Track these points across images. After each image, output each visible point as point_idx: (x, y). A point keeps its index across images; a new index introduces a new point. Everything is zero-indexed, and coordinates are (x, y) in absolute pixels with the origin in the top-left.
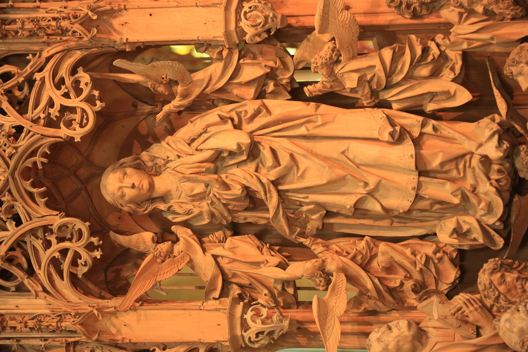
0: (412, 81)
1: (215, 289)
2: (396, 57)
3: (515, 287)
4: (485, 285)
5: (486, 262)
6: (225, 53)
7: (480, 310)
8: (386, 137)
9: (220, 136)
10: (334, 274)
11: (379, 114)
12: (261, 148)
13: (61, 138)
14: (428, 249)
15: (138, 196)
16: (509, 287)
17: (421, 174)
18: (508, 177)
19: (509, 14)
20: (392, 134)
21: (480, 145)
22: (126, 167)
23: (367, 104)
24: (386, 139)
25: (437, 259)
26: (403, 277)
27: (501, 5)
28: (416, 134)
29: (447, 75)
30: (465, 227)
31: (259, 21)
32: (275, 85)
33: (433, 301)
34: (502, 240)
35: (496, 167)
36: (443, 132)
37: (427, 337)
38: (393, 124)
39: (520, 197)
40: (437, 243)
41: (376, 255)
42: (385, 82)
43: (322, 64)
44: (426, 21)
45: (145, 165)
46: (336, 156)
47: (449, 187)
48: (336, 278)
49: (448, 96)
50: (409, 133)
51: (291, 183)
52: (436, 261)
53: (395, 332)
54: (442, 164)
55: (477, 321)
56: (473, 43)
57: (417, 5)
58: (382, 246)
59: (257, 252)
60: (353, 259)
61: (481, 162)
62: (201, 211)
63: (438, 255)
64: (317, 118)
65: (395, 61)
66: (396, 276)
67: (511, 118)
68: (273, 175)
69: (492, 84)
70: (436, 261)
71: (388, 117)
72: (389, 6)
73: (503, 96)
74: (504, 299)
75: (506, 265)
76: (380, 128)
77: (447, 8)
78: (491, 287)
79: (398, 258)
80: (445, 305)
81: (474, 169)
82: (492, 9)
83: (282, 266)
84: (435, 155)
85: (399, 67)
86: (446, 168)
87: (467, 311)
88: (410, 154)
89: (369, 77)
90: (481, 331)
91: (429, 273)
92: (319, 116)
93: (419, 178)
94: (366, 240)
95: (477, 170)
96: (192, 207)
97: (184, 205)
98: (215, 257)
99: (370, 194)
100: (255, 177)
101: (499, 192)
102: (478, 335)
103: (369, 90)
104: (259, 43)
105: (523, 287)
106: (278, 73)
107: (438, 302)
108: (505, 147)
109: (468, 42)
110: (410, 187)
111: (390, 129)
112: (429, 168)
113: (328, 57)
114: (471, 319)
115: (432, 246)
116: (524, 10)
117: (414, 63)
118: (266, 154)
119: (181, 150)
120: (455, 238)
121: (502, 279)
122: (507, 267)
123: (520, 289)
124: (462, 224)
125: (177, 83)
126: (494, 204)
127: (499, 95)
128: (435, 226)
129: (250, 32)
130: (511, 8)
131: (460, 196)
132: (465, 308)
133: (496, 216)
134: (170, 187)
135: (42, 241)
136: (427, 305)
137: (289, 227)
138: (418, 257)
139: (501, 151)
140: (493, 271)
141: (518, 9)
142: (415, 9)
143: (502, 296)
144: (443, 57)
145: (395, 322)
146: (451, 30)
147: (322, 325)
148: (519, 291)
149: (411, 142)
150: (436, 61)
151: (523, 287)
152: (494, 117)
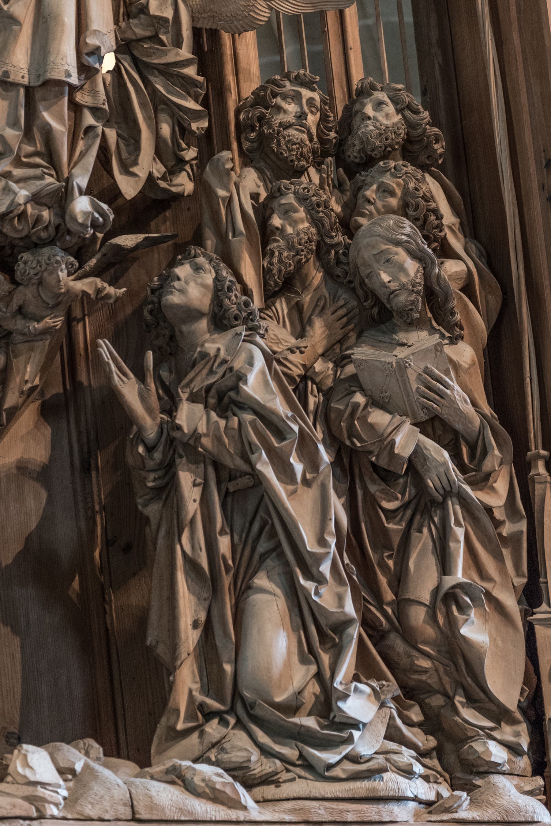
27: (286, 254)
29: (158, 169)
130: (283, 268)
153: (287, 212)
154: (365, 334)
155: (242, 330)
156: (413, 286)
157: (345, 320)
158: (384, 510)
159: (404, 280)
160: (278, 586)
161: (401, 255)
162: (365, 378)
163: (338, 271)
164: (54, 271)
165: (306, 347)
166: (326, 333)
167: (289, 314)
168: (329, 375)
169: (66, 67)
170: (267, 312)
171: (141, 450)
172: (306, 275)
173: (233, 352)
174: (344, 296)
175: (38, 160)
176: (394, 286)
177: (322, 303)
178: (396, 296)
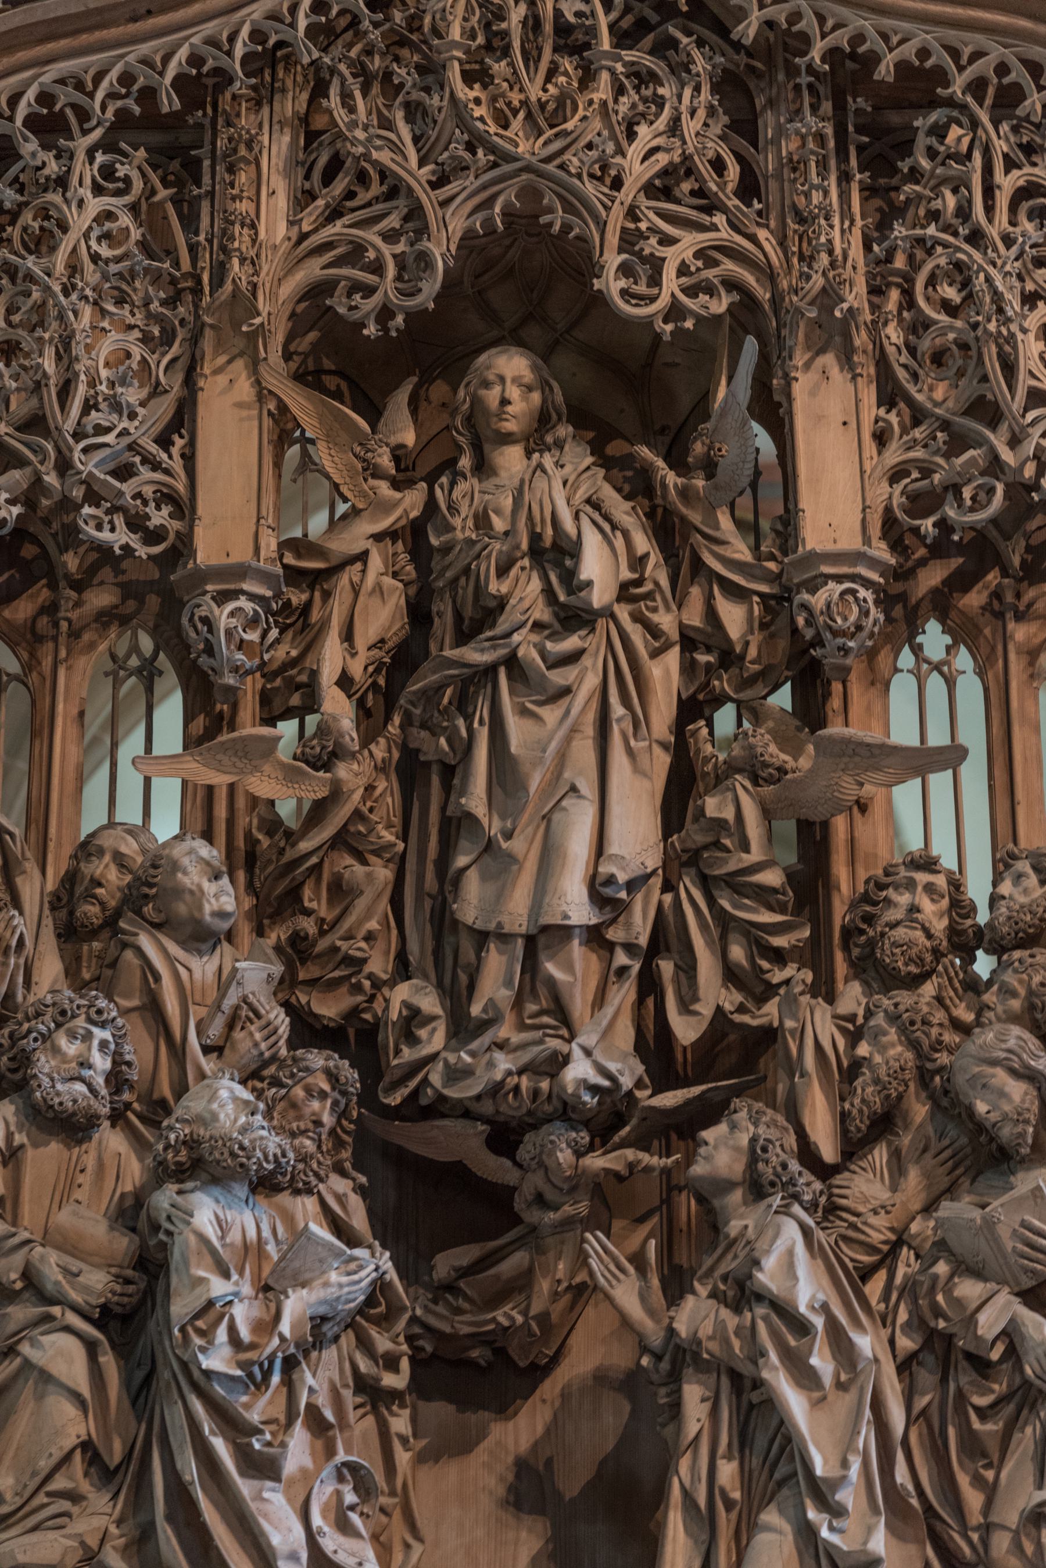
0: (720, 930)
1: (299, 556)
2: (764, 896)
3: (299, 1118)
4: (304, 1059)
5: (352, 1066)
6: (772, 565)
7: (255, 1052)
8: (605, 869)
9: (607, 549)
10: (328, 775)
11: (653, 861)
12: (583, 633)
13: (601, 254)
14: (378, 965)
15: (486, 412)
16: (300, 1103)
17: (530, 941)
18: (524, 1110)
19: (852, 1105)
20: (611, 880)
21: (588, 1053)
22: (543, 393)
23: (672, 843)
24: (601, 869)
25: (359, 982)
26: (323, 913)
27: (870, 1090)
28: (614, 934)
29: (731, 999)
30: (423, 1033)
31: (839, 621)
32: (708, 663)
33: (272, 963)
34: (398, 1100)
35: (545, 1085)
36: (616, 986)
37: (200, 953)
38: (631, 886)
39: (485, 1135)
40: (392, 983)
41: (364, 862)
42: (717, 873)
43: (751, 747)
44: (839, 956)
45: (547, 431)
46: (567, 775)
47: (504, 995)
48: (319, 778)
49: (687, 999)
50: (614, 921)
51: (512, 692)
52: (353, 980)
53: (209, 888)
54: (551, 983)
55: (233, 1048)
56: (794, 1040)
57: (871, 933)
58: (384, 874)
60: (357, 815)
61: (555, 1053)
62: (455, 529)
63: (367, 984)
64: (644, 740)
66: (324, 901)
67: (644, 1119)
68: (529, 653)
69: (710, 1085)
70: (353, 980)
71: (649, 876)
72: (867, 882)
73: (688, 1103)
74: (279, 1096)
75: (347, 1105)
76: (623, 858)
77: (864, 993)
79: (361, 905)
80: (264, 985)
81: (541, 1042)
82: (864, 1074)
83: (344, 681)
84: (569, 968)
85: (746, 901)
86: (542, 991)
87: (253, 1028)
88: (570, 914)
89: (727, 842)
90: (215, 1054)
91: (331, 966)
92: (647, 743)
93: (522, 936)
95: (536, 1049)
96: (463, 515)
97: (467, 501)
98: (363, 557)
99: (490, 846)
100: (524, 618)
101: (496, 1090)
102: (207, 1050)
103: (699, 845)
104: (795, 631)
105: (303, 1132)
106: (734, 671)
108: (587, 1098)
109: (796, 1029)
110: (505, 919)
111: (622, 877)
112: (542, 956)
113: (767, 758)
114: (238, 1035)
115: (386, 972)
116: (860, 1135)
117: (753, 930)
118: (572, 642)
119: (578, 488)
120: (400, 1012)
122: (342, 1106)
123: (298, 1127)
124: (429, 1027)
125: (710, 477)
126: (468, 1082)
127: (691, 1096)
128: (426, 977)
129: (818, 600)
131: (485, 1016)
133: (444, 1087)
134: (503, 474)
135: (398, 227)
136: (266, 954)
137: (424, 692)
138: (363, 945)
139: (577, 1088)
140: (332, 1077)
141: (861, 1121)
142: (862, 932)
143: (283, 1091)
144: (767, 991)
145: (230, 889)
146: (820, 1000)
147: (224, 747)
148: (294, 1125)
149: (594, 921)
150: (757, 976)
152: (646, 1087)
153: (878, 1033)
154: (980, 1178)
155: (777, 1201)
156: (1019, 1114)
157: (950, 1163)
158: (977, 1409)
159: (1007, 1108)
160: (789, 1521)
161: (1001, 1077)
162: (953, 1242)
163: (945, 1102)
165: (893, 1205)
167: (888, 1162)
168: (928, 1237)
170: (861, 1163)
171: (645, 1361)
172: (907, 1111)
173: (760, 1232)
174: (952, 1132)
176: (994, 1117)
177: (922, 1146)
178: (1000, 1128)
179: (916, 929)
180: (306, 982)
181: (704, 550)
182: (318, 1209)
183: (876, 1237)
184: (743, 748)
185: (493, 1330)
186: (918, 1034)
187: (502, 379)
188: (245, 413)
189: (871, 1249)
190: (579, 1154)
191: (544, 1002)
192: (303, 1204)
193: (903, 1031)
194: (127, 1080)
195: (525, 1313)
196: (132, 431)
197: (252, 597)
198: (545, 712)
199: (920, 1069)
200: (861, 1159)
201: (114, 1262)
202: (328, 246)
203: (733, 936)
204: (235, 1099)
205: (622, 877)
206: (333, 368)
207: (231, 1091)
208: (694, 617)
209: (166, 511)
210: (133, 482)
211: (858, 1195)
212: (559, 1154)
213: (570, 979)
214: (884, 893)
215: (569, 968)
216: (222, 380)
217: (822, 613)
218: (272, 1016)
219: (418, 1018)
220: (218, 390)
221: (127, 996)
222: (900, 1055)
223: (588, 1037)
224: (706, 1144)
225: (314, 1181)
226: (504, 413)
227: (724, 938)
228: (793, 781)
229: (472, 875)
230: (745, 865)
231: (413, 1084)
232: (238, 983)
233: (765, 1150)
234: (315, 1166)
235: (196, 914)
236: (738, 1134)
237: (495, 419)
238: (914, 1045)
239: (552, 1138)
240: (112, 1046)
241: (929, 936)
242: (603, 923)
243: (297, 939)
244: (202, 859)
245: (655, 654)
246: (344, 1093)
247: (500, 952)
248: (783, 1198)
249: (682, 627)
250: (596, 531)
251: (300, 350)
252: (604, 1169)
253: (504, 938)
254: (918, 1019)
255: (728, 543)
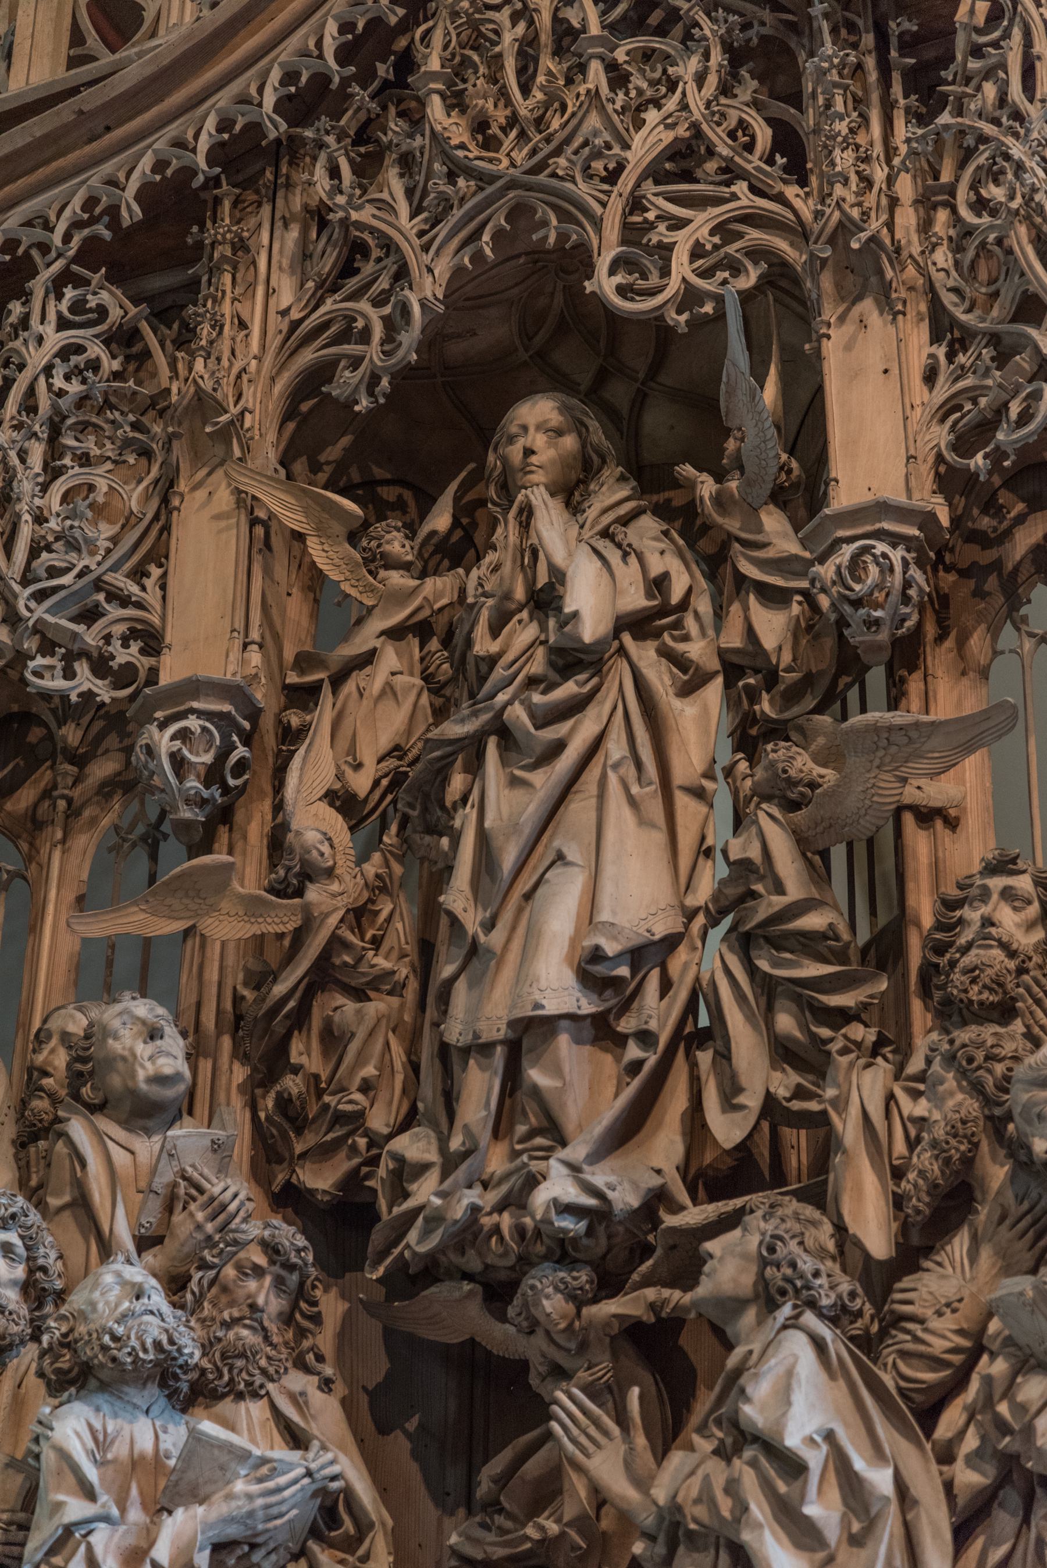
3: (232, 1304)
7: (200, 1236)
16: (231, 1285)
37: (148, 1132)
46: (556, 844)
53: (143, 1050)
54: (536, 1092)
59: (385, 742)
60: (335, 942)
65: (804, 945)
67: (674, 1247)
68: (518, 713)
75: (301, 1284)
78: (227, 1245)
80: (210, 1154)
84: (557, 1070)
85: (788, 955)
88: (544, 1002)
93: (502, 1042)
94: (394, 972)
105: (236, 1321)
107: (215, 1138)
110: (482, 1026)
112: (525, 1063)
114: (178, 1218)
117: (799, 990)
121: (252, 1269)
130: (921, 1182)
132: (202, 1199)
140: (271, 1248)
141: (919, 1200)
143: (212, 1273)
148: (226, 1315)
150: (820, 1050)
151: (236, 1321)
155: (787, 1310)
164: (538, 1304)
165: (960, 1300)
166: (999, 1265)
169: (537, 996)
175: (539, 1141)
179: (991, 947)
180: (303, 1155)
181: (741, 559)
182: (268, 1414)
183: (938, 1346)
184: (766, 769)
185: (530, 1550)
186: (981, 1072)
187: (525, 428)
188: (223, 524)
189: (935, 1362)
190: (579, 1300)
191: (533, 1120)
192: (248, 1410)
193: (963, 1073)
194: (44, 1289)
195: (558, 1521)
196: (93, 567)
197: (208, 715)
198: (537, 778)
199: (990, 1118)
200: (938, 1253)
201: (7, 1507)
202: (325, 326)
203: (780, 1003)
204: (124, 1283)
205: (611, 948)
206: (389, 476)
207: (118, 1274)
208: (733, 639)
209: (135, 647)
210: (101, 623)
211: (929, 1297)
212: (545, 1302)
213: (556, 1083)
214: (958, 913)
215: (557, 1070)
216: (201, 494)
217: (834, 583)
218: (216, 1190)
219: (407, 1169)
220: (196, 506)
221: (57, 1194)
222: (960, 1104)
223: (577, 1151)
224: (711, 1256)
225: (258, 1380)
226: (528, 465)
227: (769, 1010)
228: (825, 794)
229: (461, 987)
230: (776, 909)
231: (396, 1251)
232: (171, 1156)
233: (772, 1250)
234: (263, 1362)
235: (130, 1084)
236: (749, 1237)
237: (520, 474)
238: (977, 1089)
239: (531, 1282)
240: (21, 1250)
241: (1012, 954)
242: (608, 1011)
243: (284, 1103)
244: (138, 1018)
245: (686, 690)
246: (291, 1267)
247: (482, 1068)
248: (795, 1306)
249: (722, 653)
250: (595, 558)
251: (331, 458)
252: (615, 1316)
253: (485, 1049)
254: (980, 1056)
255: (769, 544)
